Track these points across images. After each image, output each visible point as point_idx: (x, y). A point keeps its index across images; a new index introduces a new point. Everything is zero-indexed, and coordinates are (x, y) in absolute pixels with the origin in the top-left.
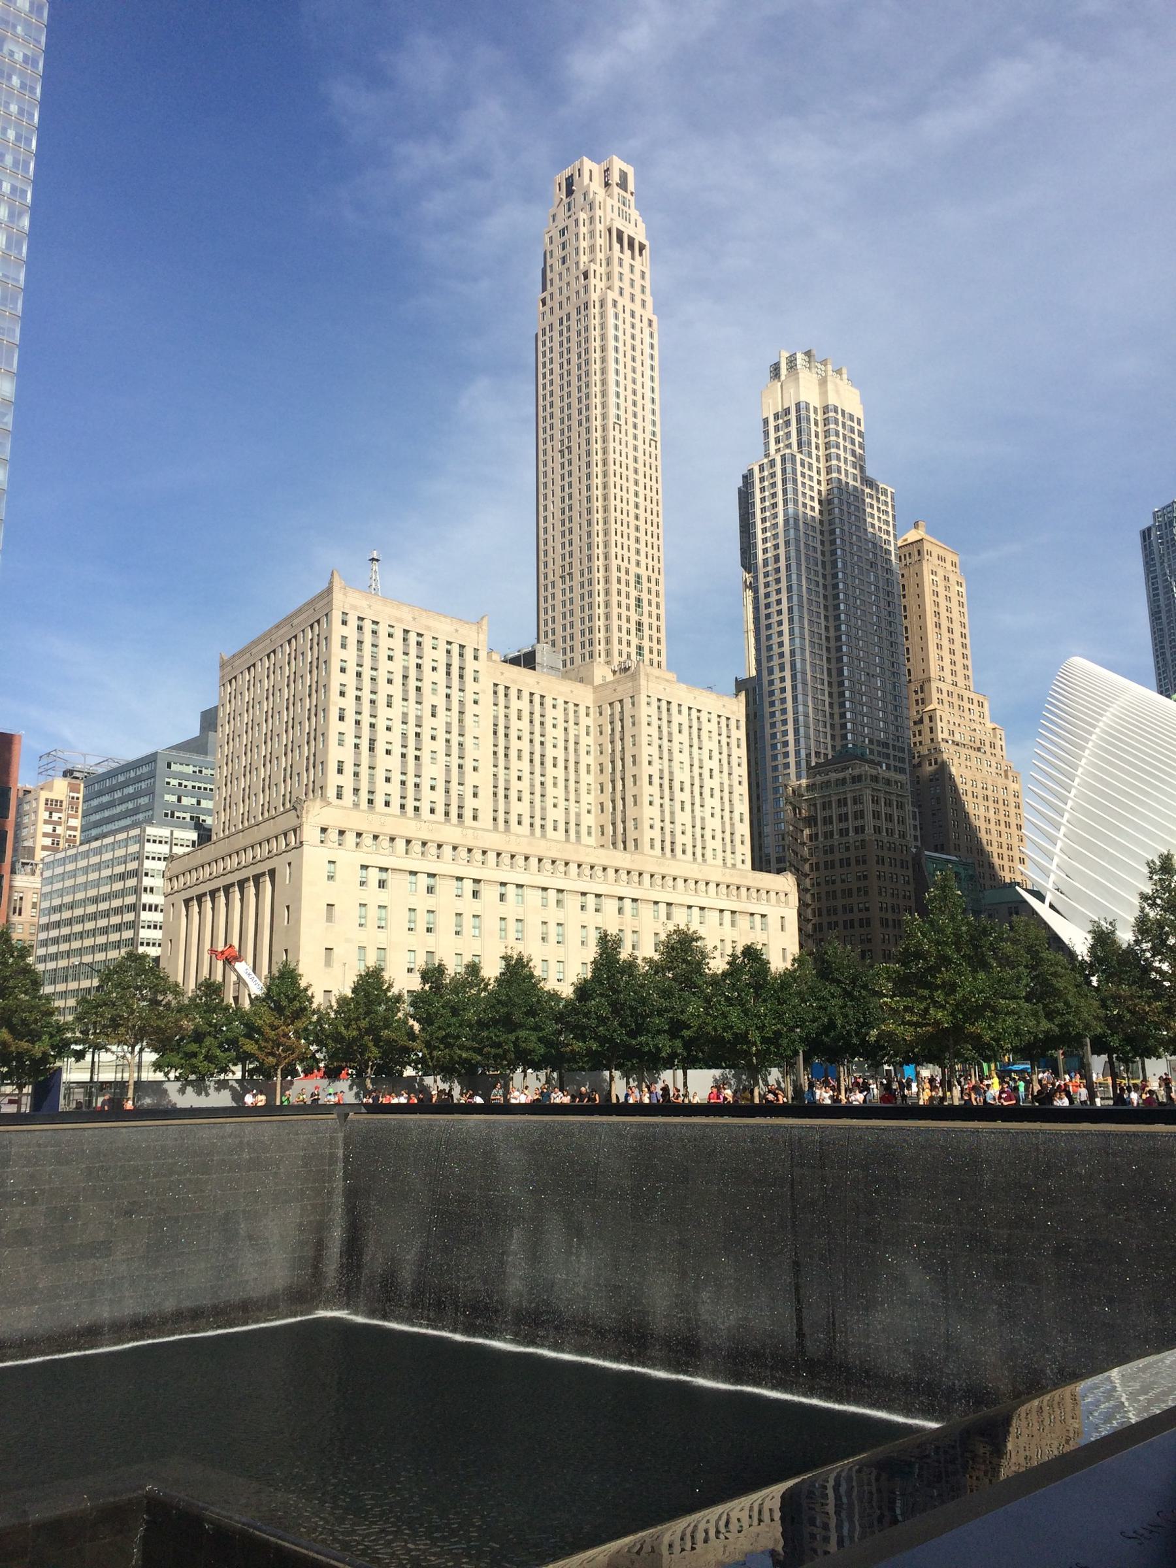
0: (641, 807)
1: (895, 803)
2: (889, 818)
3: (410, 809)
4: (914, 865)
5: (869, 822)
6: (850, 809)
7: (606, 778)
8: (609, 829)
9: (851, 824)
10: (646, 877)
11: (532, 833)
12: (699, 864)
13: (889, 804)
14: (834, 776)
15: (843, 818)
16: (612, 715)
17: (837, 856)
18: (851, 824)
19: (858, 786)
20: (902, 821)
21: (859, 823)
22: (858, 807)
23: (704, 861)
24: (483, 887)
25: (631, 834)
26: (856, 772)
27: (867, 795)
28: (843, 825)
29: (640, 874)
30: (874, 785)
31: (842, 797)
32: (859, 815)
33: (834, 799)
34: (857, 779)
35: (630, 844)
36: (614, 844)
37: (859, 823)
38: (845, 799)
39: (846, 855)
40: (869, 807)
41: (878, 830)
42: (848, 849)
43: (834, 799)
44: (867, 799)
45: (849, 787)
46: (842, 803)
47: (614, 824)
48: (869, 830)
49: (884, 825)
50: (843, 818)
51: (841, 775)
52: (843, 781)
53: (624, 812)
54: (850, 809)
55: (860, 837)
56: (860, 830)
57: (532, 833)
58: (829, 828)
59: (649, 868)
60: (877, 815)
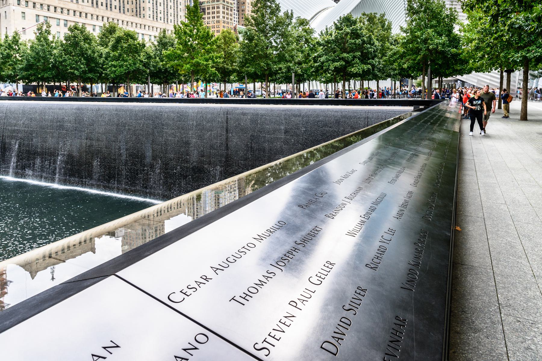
0: (146, 3)
1: (229, 9)
2: (227, 14)
4: (234, 29)
5: (221, 15)
6: (215, 10)
9: (215, 15)
10: (147, 27)
11: (107, 9)
12: (166, 24)
13: (227, 9)
15: (213, 13)
21: (218, 15)
22: (218, 10)
23: (168, 23)
25: (142, 12)
27: (221, 6)
28: (213, 15)
29: (145, 26)
30: (223, 3)
31: (213, 6)
32: (218, 12)
33: (211, 7)
35: (142, 16)
36: (137, 15)
37: (218, 15)
38: (214, 7)
40: (221, 10)
43: (211, 7)
44: (221, 6)
46: (213, 8)
47: (136, 8)
48: (221, 17)
49: (226, 16)
50: (213, 13)
55: (218, 19)
56: (219, 17)
57: (107, 9)
58: (209, 16)
59: (148, 23)
60: (224, 13)
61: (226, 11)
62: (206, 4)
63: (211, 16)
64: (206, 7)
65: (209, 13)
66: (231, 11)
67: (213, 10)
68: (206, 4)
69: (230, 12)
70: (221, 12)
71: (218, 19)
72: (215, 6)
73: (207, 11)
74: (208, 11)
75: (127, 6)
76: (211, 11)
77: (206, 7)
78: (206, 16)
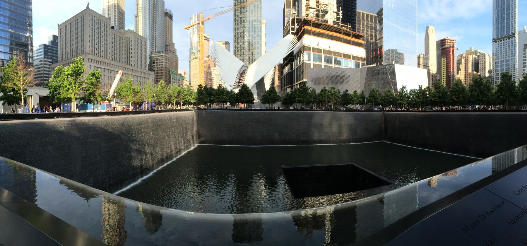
3: (99, 56)
5: (164, 63)
6: (161, 61)
7: (126, 52)
8: (126, 62)
9: (161, 64)
14: (158, 55)
15: (160, 62)
16: (127, 40)
17: (158, 69)
18: (161, 64)
19: (162, 57)
20: (168, 64)
21: (162, 63)
24: (112, 71)
25: (131, 63)
26: (162, 54)
33: (158, 59)
34: (162, 56)
35: (130, 65)
37: (162, 63)
39: (160, 69)
41: (165, 65)
42: (157, 68)
43: (158, 59)
45: (161, 57)
48: (164, 65)
49: (166, 64)
50: (160, 62)
51: (159, 55)
52: (160, 56)
53: (129, 59)
54: (161, 61)
55: (162, 66)
56: (162, 65)
58: (157, 64)
59: (135, 69)
61: (166, 61)
62: (155, 58)
63: (158, 64)
64: (155, 59)
65: (157, 63)
66: (168, 61)
67: (160, 61)
68: (155, 58)
69: (167, 62)
70: (164, 62)
71: (162, 66)
72: (161, 59)
73: (155, 62)
74: (157, 61)
75: (122, 60)
76: (158, 61)
77: (155, 59)
78: (155, 64)
